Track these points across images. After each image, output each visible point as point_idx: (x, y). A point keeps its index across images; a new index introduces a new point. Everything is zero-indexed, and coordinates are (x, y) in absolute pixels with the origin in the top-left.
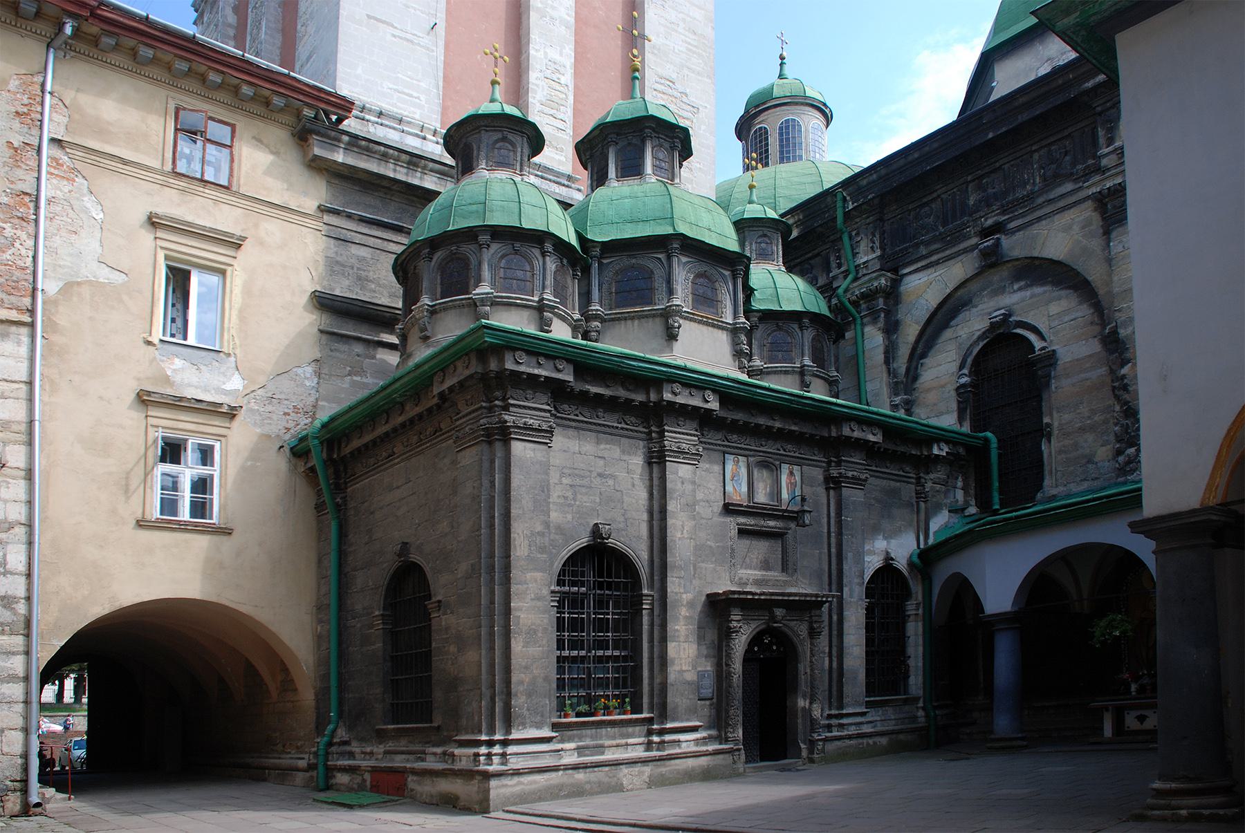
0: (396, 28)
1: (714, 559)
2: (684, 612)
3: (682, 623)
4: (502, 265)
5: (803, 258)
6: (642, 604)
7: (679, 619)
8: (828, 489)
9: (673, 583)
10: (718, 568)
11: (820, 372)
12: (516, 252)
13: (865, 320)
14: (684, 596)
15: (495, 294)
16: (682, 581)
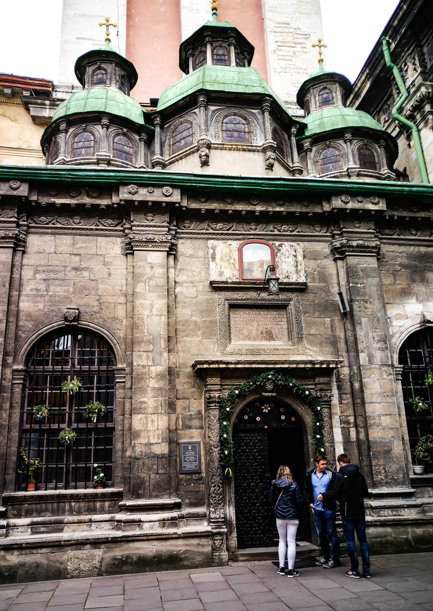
0: (95, 40)
1: (200, 333)
2: (153, 383)
3: (150, 395)
4: (75, 141)
5: (382, 103)
6: (116, 378)
7: (146, 391)
8: (335, 260)
9: (140, 357)
10: (205, 341)
11: (368, 172)
12: (85, 130)
13: (420, 127)
14: (153, 369)
15: (67, 160)
16: (150, 354)
